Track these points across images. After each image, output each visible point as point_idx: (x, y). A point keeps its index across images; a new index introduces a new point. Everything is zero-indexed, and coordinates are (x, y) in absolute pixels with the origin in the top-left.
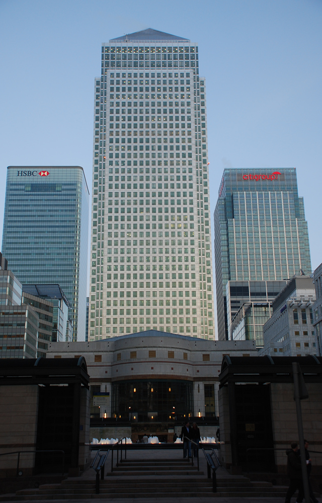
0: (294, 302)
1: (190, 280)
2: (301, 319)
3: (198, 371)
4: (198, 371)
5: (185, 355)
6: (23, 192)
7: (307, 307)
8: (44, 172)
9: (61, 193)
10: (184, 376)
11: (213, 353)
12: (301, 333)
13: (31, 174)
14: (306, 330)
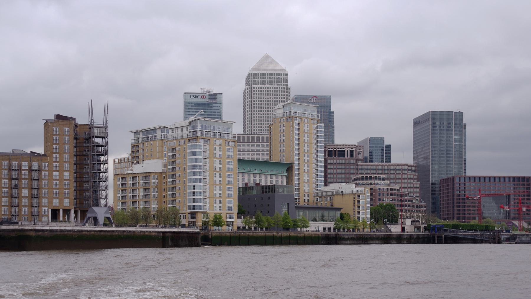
6: (193, 108)
8: (203, 96)
9: (212, 108)
13: (197, 97)
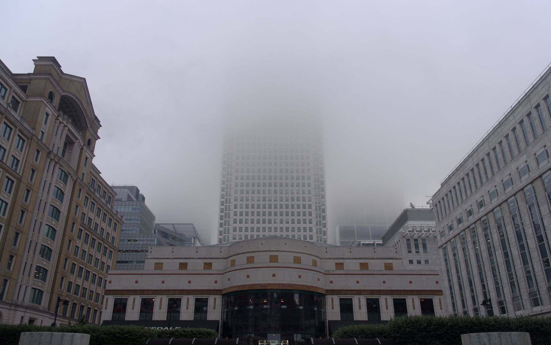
0: (407, 232)
1: (307, 218)
2: (414, 248)
3: (331, 282)
4: (331, 282)
5: (315, 263)
7: (419, 237)
10: (316, 287)
11: (347, 261)
12: (415, 262)
14: (420, 259)
